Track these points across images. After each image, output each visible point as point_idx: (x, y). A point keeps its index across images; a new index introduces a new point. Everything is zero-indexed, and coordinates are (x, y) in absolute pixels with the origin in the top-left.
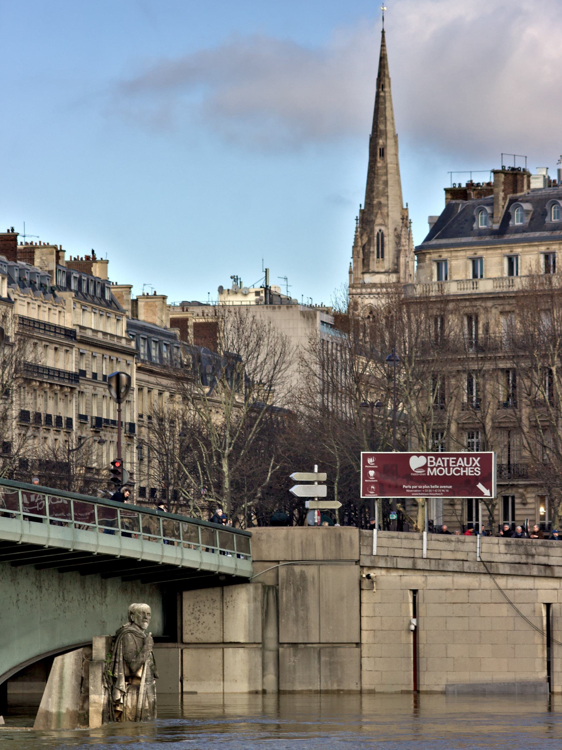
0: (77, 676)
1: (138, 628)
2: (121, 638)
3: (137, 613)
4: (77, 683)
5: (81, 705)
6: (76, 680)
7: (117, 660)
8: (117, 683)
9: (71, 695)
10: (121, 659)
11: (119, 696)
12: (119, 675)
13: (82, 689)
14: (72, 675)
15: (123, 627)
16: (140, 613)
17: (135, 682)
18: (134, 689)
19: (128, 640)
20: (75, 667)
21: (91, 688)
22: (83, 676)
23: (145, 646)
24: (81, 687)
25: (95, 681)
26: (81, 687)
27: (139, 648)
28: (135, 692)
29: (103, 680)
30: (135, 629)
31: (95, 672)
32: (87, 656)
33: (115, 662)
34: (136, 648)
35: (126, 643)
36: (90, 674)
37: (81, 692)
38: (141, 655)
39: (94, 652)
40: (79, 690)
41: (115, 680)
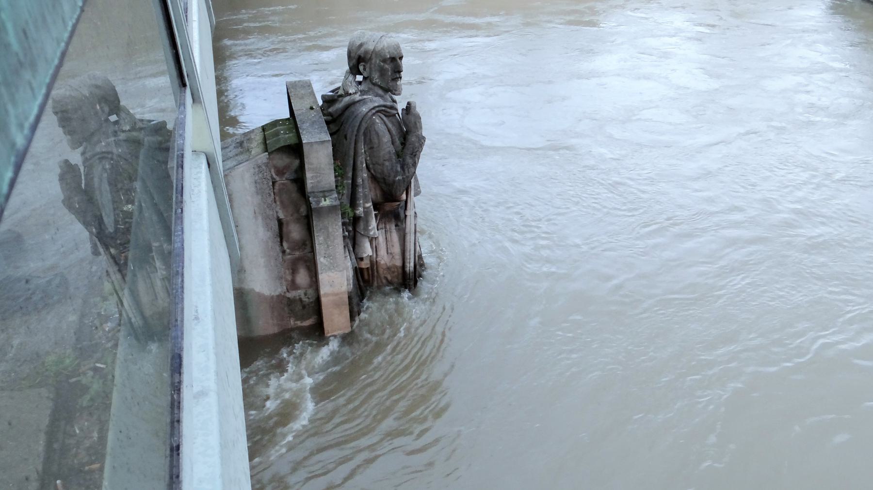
0: (266, 218)
1: (380, 92)
2: (362, 131)
3: (376, 61)
4: (269, 234)
5: (289, 278)
6: (267, 227)
7: (360, 181)
8: (361, 226)
9: (262, 261)
10: (365, 175)
11: (367, 250)
12: (364, 208)
13: (285, 245)
14: (256, 218)
15: (348, 94)
16: (384, 61)
17: (388, 207)
18: (390, 221)
19: (377, 134)
20: (257, 199)
21: (321, 260)
22: (281, 216)
23: (412, 139)
24: (281, 242)
25: (328, 246)
26: (281, 242)
27: (398, 142)
28: (393, 227)
29: (344, 237)
30: (382, 102)
31: (326, 228)
32: (280, 172)
33: (354, 185)
34: (393, 143)
35: (376, 141)
36: (316, 234)
37: (284, 252)
38: (409, 160)
39: (309, 175)
40: (278, 248)
41: (356, 220)
